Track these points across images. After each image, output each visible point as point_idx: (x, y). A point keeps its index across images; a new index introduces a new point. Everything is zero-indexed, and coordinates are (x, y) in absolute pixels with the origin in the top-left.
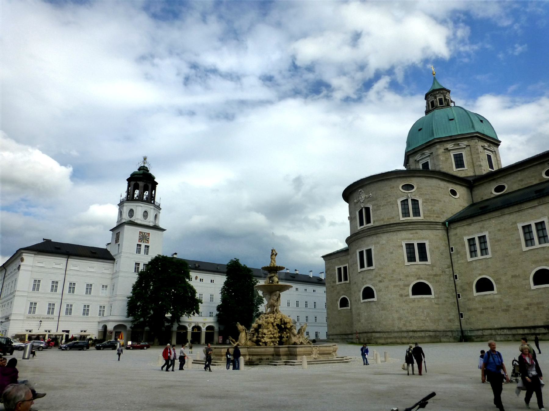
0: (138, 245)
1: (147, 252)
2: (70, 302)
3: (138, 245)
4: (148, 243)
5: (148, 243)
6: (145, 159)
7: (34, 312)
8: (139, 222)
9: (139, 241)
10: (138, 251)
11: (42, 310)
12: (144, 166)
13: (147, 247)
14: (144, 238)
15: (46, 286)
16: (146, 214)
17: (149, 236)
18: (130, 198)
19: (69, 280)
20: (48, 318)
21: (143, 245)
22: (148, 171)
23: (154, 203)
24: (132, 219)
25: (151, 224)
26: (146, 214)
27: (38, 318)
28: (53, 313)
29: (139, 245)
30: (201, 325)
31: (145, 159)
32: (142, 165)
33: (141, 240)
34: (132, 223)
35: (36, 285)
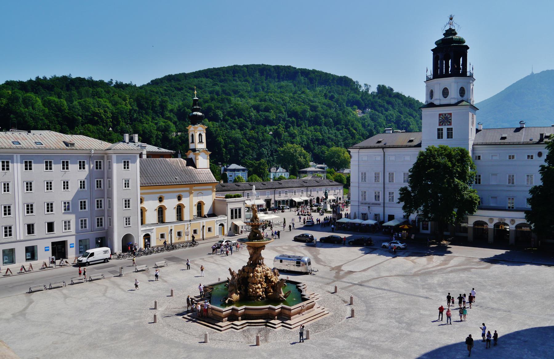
0: (438, 129)
1: (450, 135)
2: (391, 191)
3: (438, 129)
4: (451, 125)
5: (451, 125)
6: (451, 19)
7: (365, 199)
8: (437, 103)
9: (440, 125)
10: (440, 136)
11: (370, 198)
12: (450, 29)
13: (450, 131)
14: (445, 119)
15: (371, 176)
16: (445, 93)
17: (451, 116)
18: (437, 74)
19: (388, 170)
20: (376, 204)
21: (445, 128)
22: (456, 34)
23: (464, 74)
24: (432, 101)
25: (453, 102)
26: (445, 93)
27: (369, 204)
28: (379, 200)
29: (440, 131)
30: (507, 221)
31: (451, 19)
32: (447, 28)
33: (441, 123)
34: (431, 105)
35: (364, 177)
